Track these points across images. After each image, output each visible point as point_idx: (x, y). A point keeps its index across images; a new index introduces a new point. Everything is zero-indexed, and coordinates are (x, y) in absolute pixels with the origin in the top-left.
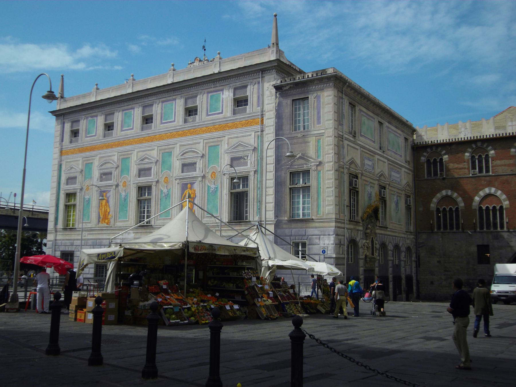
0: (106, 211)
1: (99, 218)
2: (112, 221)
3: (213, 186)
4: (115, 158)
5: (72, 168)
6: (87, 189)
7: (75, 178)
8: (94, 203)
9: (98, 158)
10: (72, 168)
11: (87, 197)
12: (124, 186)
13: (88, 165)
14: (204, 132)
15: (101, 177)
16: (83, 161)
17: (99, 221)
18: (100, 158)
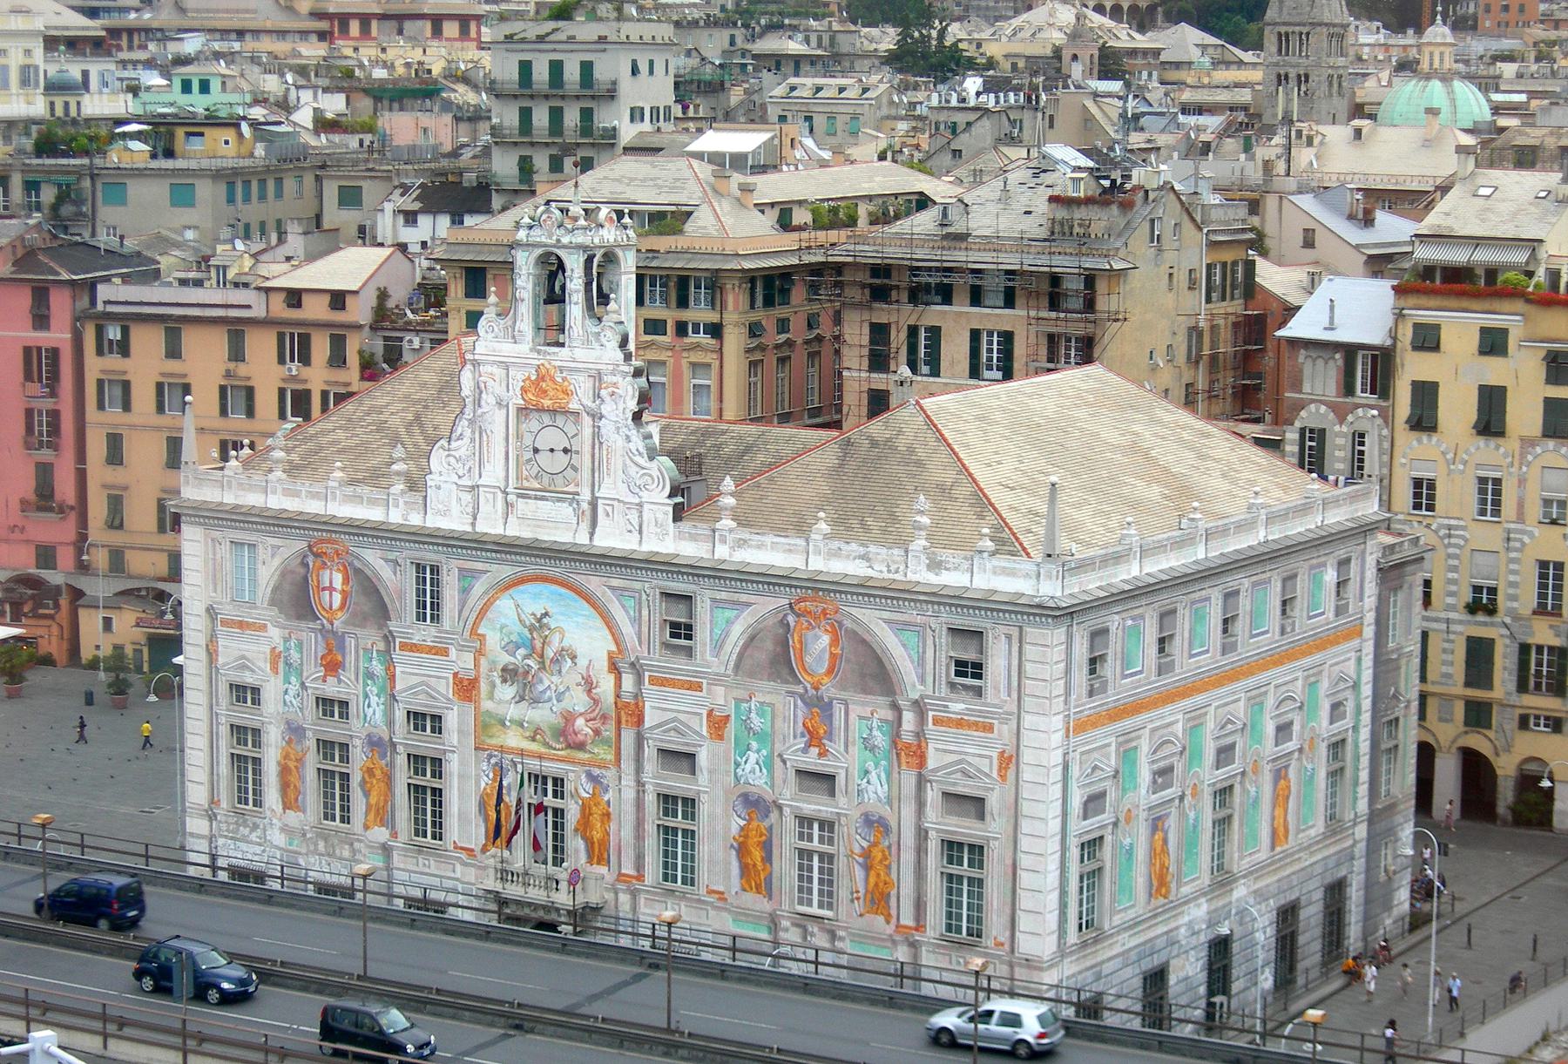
0: (1162, 866)
1: (1151, 885)
2: (1173, 886)
3: (1309, 767)
4: (1179, 728)
5: (1095, 768)
6: (1128, 820)
7: (1103, 795)
8: (1141, 853)
9: (1147, 731)
10: (1095, 768)
11: (1128, 840)
12: (1193, 795)
13: (1127, 753)
14: (1305, 654)
15: (1155, 782)
16: (1119, 745)
17: (1151, 895)
18: (1153, 730)
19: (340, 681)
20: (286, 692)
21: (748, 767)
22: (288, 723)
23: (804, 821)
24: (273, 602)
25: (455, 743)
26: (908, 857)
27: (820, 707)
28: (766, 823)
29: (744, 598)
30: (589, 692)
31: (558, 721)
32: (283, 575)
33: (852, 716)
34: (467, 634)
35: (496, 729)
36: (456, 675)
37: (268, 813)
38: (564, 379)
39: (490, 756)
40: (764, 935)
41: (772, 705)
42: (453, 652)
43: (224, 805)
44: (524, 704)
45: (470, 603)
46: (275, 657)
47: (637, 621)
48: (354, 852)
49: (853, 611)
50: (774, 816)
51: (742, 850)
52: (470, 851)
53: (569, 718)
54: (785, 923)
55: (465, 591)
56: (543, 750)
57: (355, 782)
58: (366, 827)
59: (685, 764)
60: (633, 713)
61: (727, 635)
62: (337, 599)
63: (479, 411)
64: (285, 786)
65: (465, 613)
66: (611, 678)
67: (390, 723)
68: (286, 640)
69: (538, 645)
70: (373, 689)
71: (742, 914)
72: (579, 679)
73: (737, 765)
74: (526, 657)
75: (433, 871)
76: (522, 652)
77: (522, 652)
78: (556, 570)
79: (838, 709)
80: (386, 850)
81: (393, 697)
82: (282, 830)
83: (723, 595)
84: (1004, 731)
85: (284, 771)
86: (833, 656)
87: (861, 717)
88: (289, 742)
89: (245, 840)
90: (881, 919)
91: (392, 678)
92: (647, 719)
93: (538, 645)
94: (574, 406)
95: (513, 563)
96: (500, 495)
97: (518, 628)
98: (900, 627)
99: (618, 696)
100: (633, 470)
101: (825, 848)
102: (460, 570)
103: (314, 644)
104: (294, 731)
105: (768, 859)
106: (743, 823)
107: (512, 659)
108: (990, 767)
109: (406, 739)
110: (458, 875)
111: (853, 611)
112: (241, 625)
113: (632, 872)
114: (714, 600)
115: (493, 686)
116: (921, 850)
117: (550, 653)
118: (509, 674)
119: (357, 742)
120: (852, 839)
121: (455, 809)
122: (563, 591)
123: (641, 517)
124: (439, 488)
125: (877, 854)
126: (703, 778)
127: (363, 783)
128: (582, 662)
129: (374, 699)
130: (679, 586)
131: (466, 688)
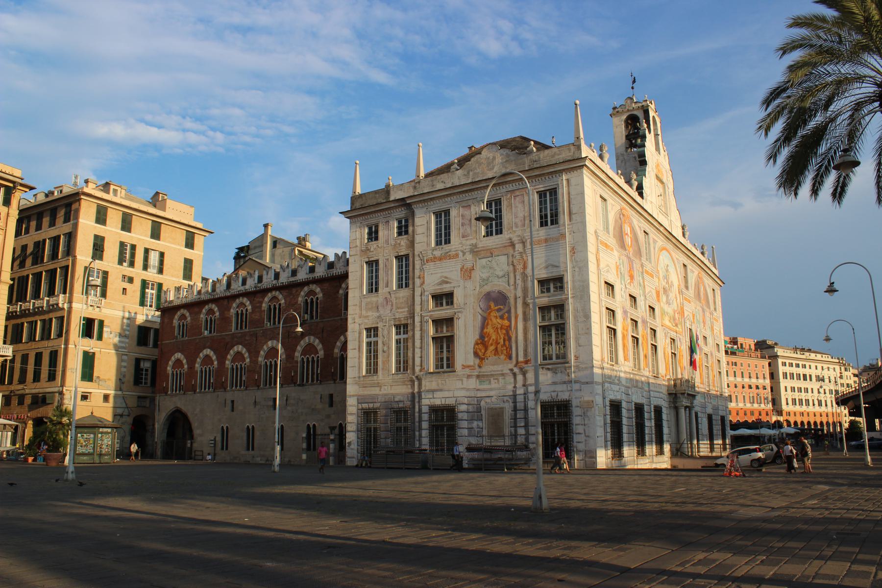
60: (682, 312)
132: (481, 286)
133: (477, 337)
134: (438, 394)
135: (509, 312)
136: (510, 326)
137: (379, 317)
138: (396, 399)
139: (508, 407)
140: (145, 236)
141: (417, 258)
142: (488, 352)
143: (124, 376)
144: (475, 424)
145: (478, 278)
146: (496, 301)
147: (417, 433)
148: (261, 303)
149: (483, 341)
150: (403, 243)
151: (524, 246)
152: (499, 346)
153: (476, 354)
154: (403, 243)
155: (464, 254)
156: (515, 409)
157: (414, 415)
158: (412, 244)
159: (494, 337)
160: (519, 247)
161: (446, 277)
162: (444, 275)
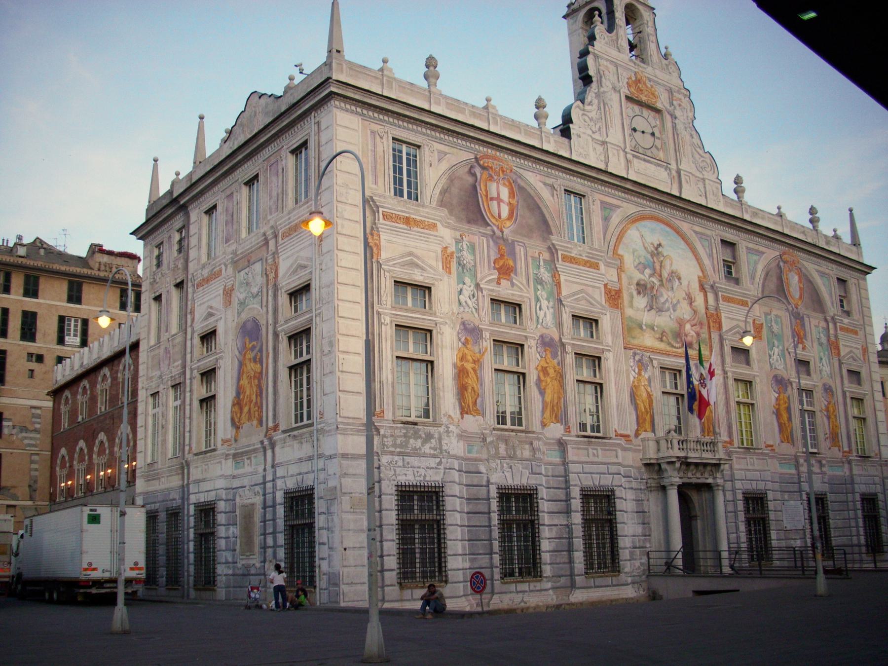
19: (513, 284)
20: (460, 292)
21: (775, 357)
22: (463, 324)
23: (801, 390)
24: (442, 203)
25: (610, 343)
26: (841, 408)
27: (798, 318)
28: (787, 395)
29: (761, 249)
30: (691, 304)
31: (674, 325)
32: (451, 180)
33: (812, 326)
34: (610, 253)
35: (637, 332)
36: (606, 285)
37: (444, 420)
38: (652, 86)
39: (635, 354)
40: (793, 471)
41: (780, 317)
42: (602, 266)
43: (389, 415)
44: (653, 312)
45: (611, 229)
46: (447, 258)
47: (711, 256)
48: (534, 450)
49: (804, 263)
50: (789, 389)
51: (778, 414)
52: (627, 436)
53: (681, 323)
54: (801, 461)
55: (606, 219)
56: (668, 348)
57: (532, 378)
58: (544, 425)
59: (742, 357)
60: (714, 320)
61: (756, 272)
62: (505, 211)
63: (602, 90)
64: (462, 390)
65: (608, 237)
66: (702, 294)
67: (559, 325)
68: (458, 241)
69: (658, 268)
70: (543, 294)
71: (783, 460)
72: (684, 295)
73: (770, 356)
74: (651, 276)
75: (600, 459)
76: (648, 272)
77: (648, 272)
78: (665, 213)
79: (806, 319)
80: (562, 445)
81: (561, 301)
82: (460, 437)
83: (751, 246)
84: (861, 333)
85: (461, 373)
86: (800, 288)
87: (814, 325)
88: (465, 344)
89: (416, 453)
90: (837, 448)
91: (558, 285)
92: (723, 325)
93: (658, 268)
94: (659, 105)
95: (637, 204)
96: (622, 153)
97: (643, 253)
98: (822, 274)
99: (707, 308)
100: (697, 156)
101: (809, 408)
102: (602, 202)
103: (486, 250)
104: (470, 332)
105: (790, 419)
106: (776, 395)
107: (642, 277)
108: (859, 353)
109: (575, 338)
110: (620, 460)
111: (804, 263)
112: (407, 221)
113: (727, 439)
114: (747, 248)
115: (632, 297)
116: (845, 404)
117: (665, 274)
118: (642, 288)
119: (533, 343)
120: (820, 402)
121: (614, 401)
122: (668, 229)
123: (705, 187)
124: (579, 136)
125: (831, 409)
126: (755, 364)
127: (539, 381)
128: (685, 283)
129: (544, 303)
130: (730, 235)
131: (614, 297)
132: (239, 314)
133: (234, 394)
134: (205, 486)
135: (261, 351)
136: (261, 373)
137: (161, 377)
138: (171, 497)
139: (258, 500)
140: (60, 300)
141: (190, 284)
142: (243, 415)
143: (36, 482)
144: (232, 529)
145: (237, 301)
146: (250, 331)
147: (186, 547)
148: (117, 372)
149: (238, 403)
150: (180, 266)
151: (277, 242)
152: (252, 405)
153: (232, 419)
154: (180, 266)
155: (226, 266)
156: (265, 507)
157: (183, 520)
158: (187, 261)
159: (248, 393)
160: (272, 243)
161: (211, 307)
162: (210, 303)
